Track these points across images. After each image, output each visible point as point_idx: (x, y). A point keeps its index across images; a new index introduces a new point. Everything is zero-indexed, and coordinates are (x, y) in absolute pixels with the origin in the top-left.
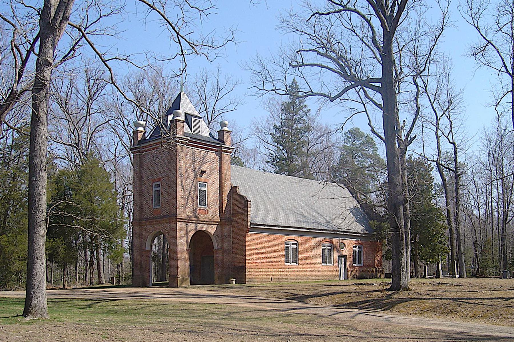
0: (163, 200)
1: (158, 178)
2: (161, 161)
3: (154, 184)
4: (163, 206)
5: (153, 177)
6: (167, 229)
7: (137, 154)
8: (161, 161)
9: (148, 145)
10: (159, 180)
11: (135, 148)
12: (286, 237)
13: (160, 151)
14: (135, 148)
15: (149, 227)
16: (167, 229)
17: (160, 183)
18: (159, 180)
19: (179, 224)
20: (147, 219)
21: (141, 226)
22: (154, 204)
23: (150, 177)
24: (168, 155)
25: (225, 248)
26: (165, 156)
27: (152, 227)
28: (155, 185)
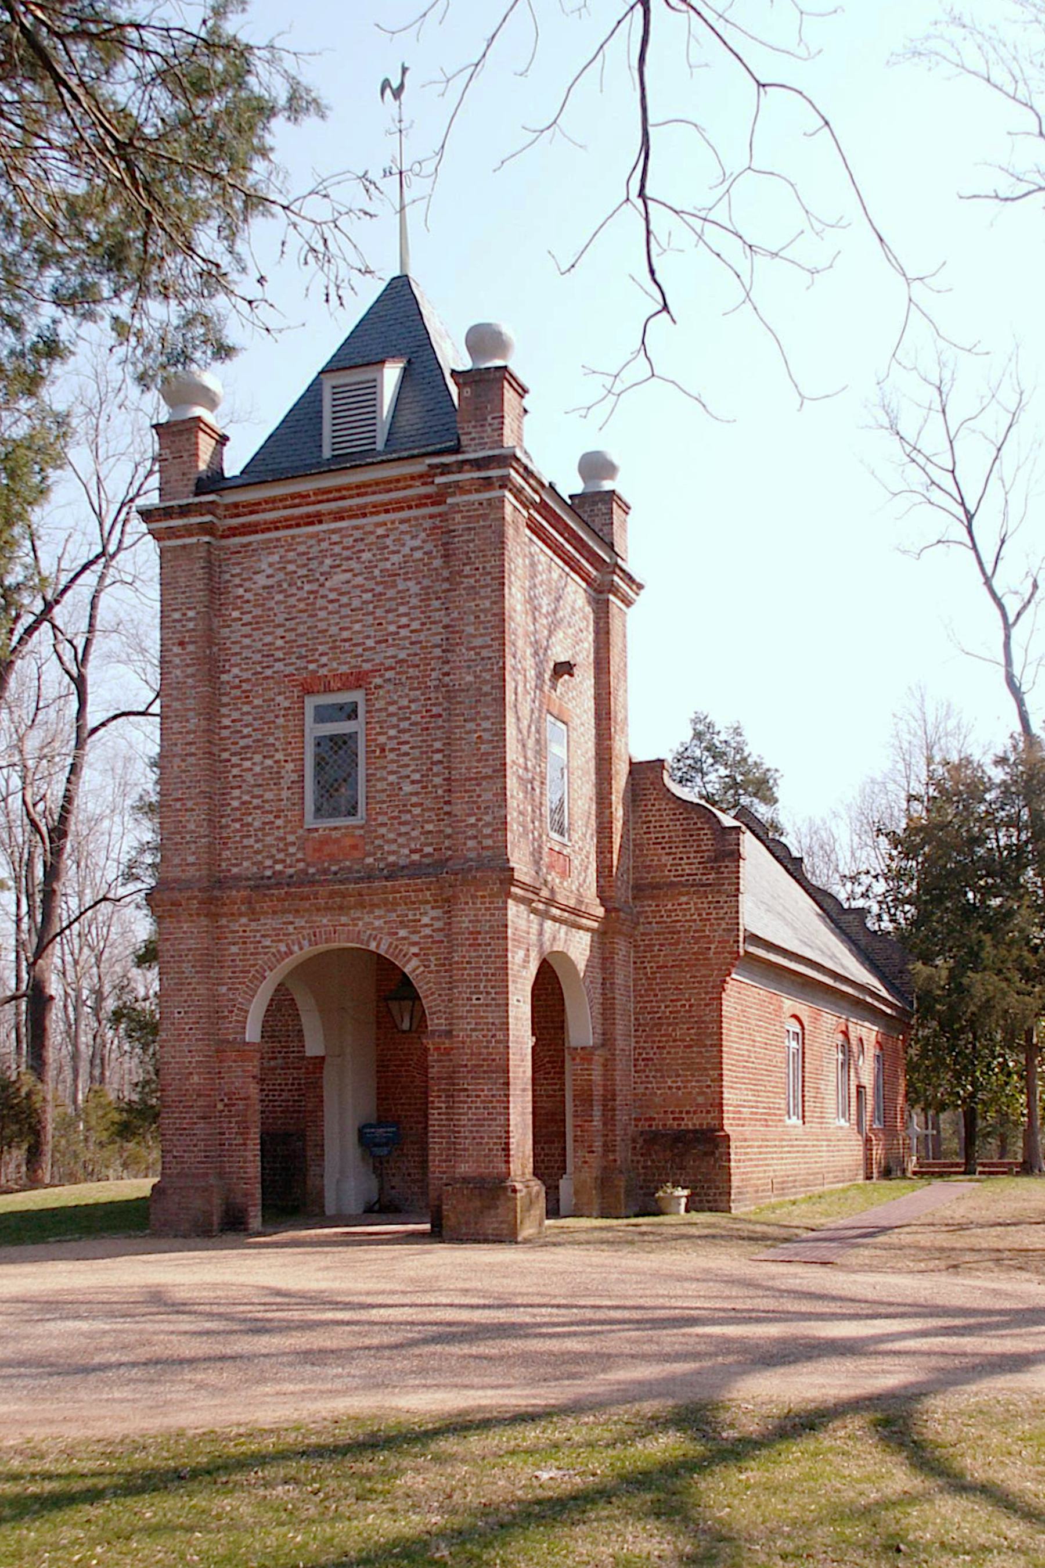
0: (380, 786)
1: (344, 669)
2: (370, 585)
3: (311, 703)
4: (382, 819)
5: (300, 663)
6: (415, 938)
7: (193, 540)
8: (370, 585)
9: (273, 500)
10: (357, 680)
11: (184, 511)
12: (790, 1004)
13: (358, 534)
14: (184, 511)
15: (270, 923)
16: (415, 938)
17: (357, 696)
18: (357, 680)
19: (514, 909)
20: (261, 885)
21: (214, 917)
22: (309, 806)
23: (279, 666)
24: (418, 555)
25: (620, 1043)
26: (395, 558)
27: (300, 922)
28: (317, 708)
